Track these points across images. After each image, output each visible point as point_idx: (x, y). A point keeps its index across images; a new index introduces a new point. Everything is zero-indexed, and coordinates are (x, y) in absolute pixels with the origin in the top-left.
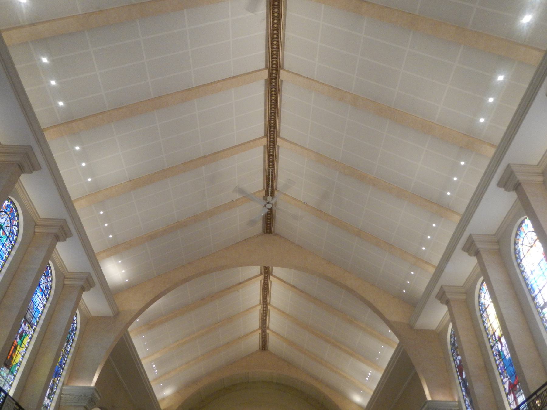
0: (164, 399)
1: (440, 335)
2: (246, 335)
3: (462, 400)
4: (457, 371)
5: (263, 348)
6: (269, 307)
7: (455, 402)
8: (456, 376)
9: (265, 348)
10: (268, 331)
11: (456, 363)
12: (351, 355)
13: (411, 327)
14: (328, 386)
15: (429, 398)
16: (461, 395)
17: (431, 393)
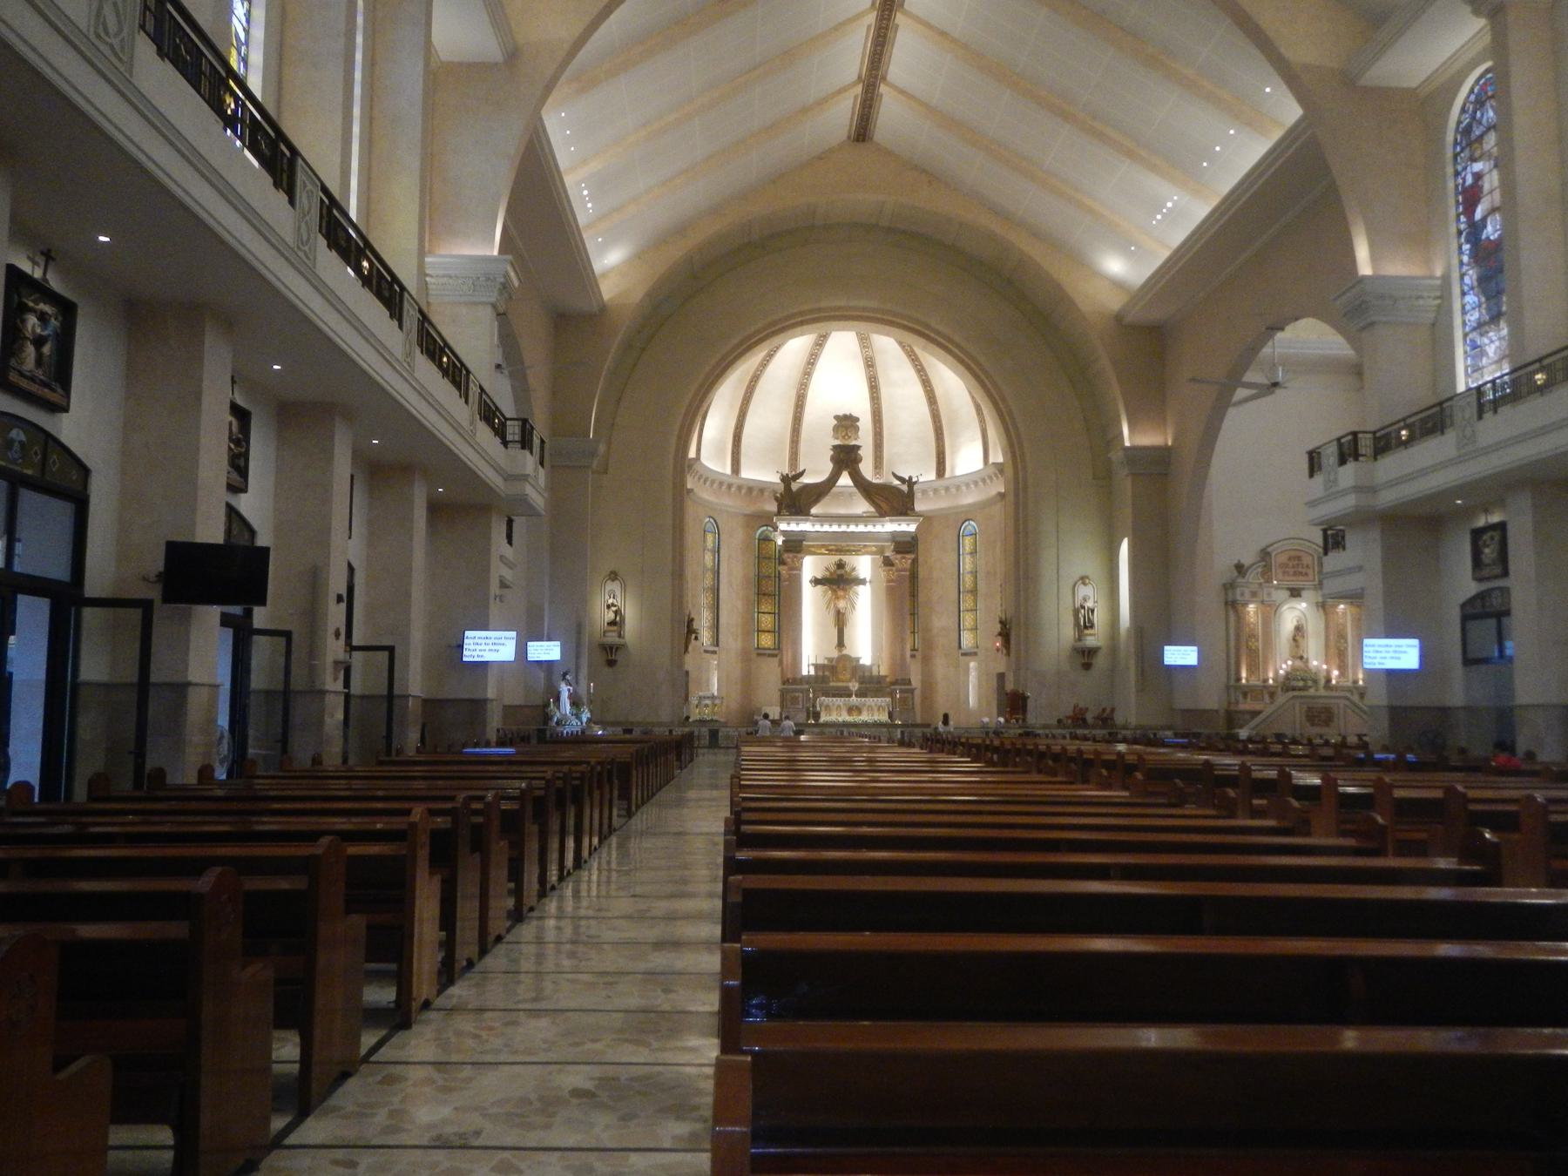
0: (604, 275)
1: (1431, 101)
2: (822, 102)
3: (1455, 275)
4: (1457, 201)
5: (859, 135)
6: (899, 18)
7: (1432, 277)
8: (1452, 213)
9: (864, 135)
10: (883, 89)
11: (1460, 181)
12: (1130, 154)
13: (1348, 81)
14: (1036, 234)
15: (1365, 268)
16: (1455, 262)
17: (1375, 259)
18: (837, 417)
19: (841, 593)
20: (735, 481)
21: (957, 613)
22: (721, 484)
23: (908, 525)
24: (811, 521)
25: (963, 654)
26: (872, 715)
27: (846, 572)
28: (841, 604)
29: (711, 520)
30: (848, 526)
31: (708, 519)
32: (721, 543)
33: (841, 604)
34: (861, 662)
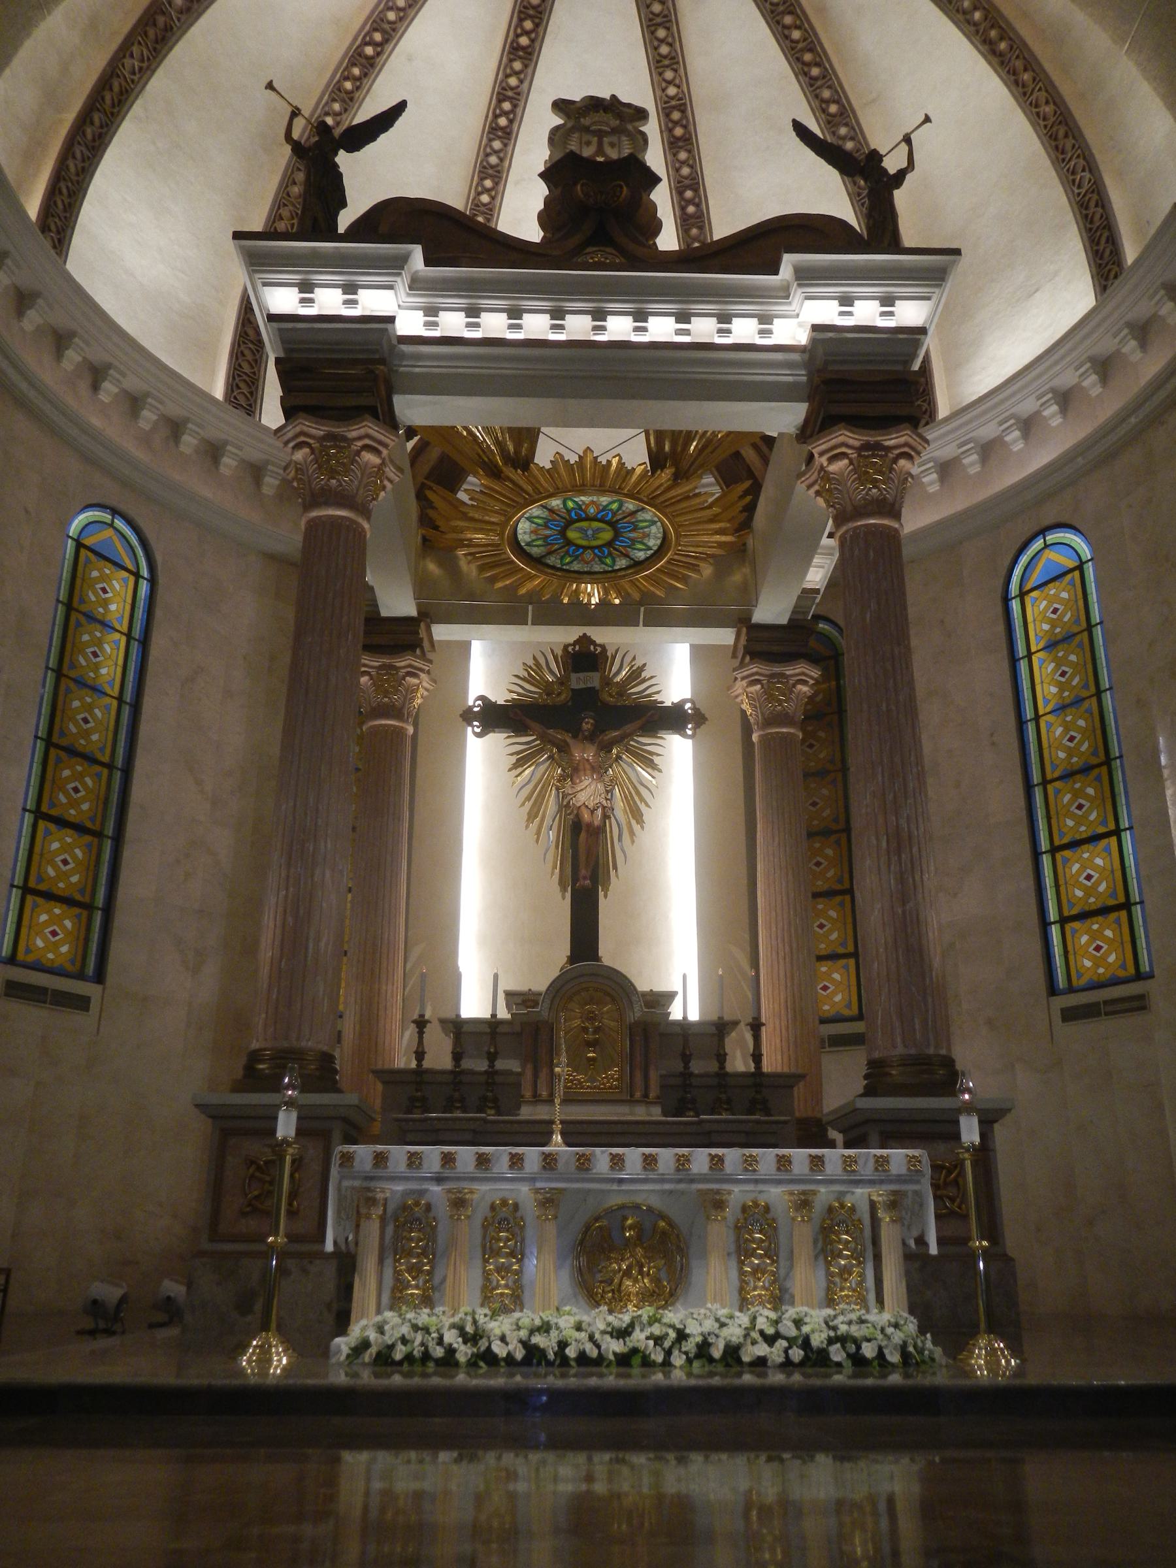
18: (560, 106)
19: (585, 753)
20: (229, 426)
21: (1028, 862)
22: (175, 428)
23: (888, 301)
24: (416, 284)
25: (1069, 1015)
26: (779, 1299)
27: (607, 682)
28: (588, 792)
29: (119, 523)
30: (599, 315)
31: (107, 517)
32: (159, 613)
33: (588, 792)
34: (676, 1012)
